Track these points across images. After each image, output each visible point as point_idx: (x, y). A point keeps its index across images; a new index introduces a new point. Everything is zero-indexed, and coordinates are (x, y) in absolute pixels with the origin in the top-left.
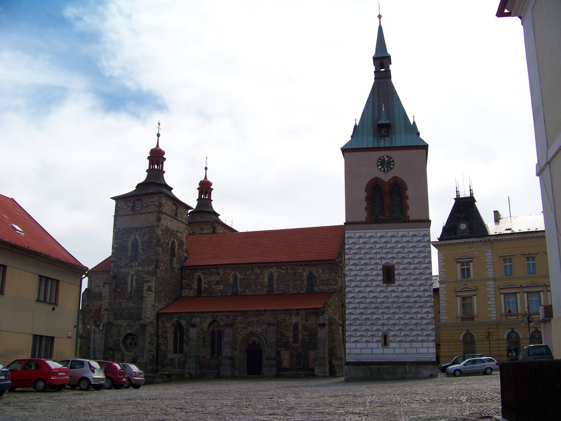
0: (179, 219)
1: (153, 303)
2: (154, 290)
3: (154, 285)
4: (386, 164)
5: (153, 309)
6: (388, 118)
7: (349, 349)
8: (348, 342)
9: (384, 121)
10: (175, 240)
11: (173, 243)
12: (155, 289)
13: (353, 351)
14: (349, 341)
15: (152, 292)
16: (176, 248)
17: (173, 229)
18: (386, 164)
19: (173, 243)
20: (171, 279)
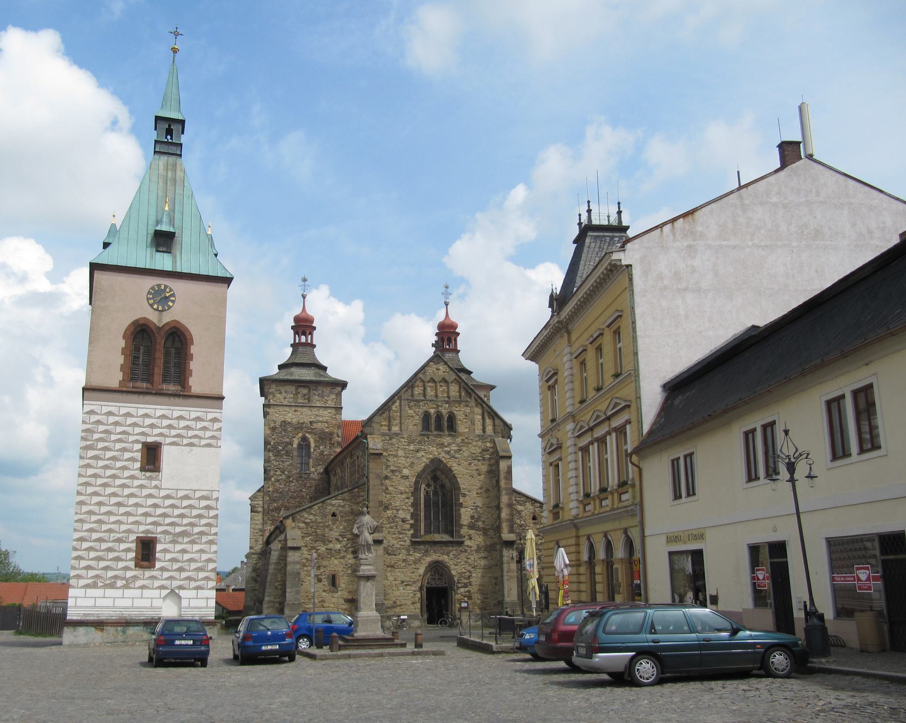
0: (318, 404)
1: (260, 527)
2: (260, 509)
3: (261, 503)
4: (161, 299)
5: (261, 535)
6: (172, 222)
7: (74, 599)
8: (73, 587)
9: (165, 228)
10: (307, 435)
11: (304, 439)
12: (263, 508)
13: (80, 602)
14: (75, 585)
15: (258, 512)
16: (313, 445)
17: (301, 421)
18: (161, 299)
19: (304, 439)
20: (301, 490)
